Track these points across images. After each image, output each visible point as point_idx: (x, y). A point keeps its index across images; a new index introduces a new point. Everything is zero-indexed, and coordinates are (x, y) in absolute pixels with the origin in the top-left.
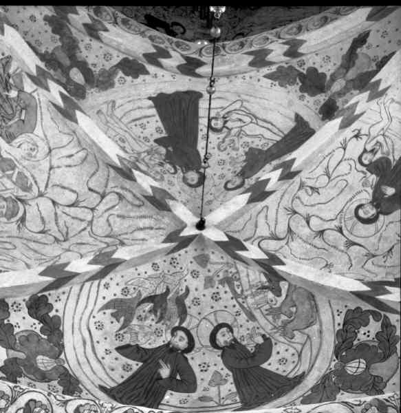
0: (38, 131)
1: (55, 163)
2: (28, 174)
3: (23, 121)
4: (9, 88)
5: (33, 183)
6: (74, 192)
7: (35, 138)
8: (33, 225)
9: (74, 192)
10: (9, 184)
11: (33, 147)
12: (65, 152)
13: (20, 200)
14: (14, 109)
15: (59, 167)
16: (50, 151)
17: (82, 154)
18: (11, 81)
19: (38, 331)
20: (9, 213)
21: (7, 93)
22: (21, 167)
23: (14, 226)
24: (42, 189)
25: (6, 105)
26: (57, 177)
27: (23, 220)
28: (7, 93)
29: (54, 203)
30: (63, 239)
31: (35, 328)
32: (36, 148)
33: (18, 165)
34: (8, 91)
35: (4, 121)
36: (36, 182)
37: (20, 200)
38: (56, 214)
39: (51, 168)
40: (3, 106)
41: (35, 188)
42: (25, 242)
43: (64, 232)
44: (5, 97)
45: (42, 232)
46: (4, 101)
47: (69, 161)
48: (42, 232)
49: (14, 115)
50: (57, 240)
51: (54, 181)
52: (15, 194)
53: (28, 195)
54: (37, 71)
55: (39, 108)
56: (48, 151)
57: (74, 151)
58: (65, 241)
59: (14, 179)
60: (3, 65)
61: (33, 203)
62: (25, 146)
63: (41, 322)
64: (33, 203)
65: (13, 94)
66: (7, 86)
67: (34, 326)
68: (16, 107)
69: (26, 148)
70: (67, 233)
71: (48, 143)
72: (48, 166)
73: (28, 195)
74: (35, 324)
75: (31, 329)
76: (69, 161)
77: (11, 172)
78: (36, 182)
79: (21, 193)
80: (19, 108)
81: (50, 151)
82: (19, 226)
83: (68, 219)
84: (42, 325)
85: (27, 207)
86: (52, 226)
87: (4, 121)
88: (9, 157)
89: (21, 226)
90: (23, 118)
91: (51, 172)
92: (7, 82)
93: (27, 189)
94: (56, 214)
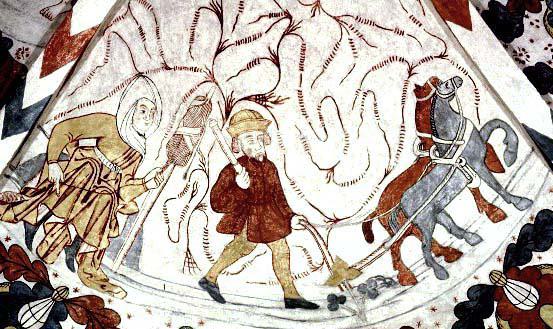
0: (109, 106)
1: (157, 62)
2: (184, 108)
3: (98, 139)
4: (46, 185)
5: (193, 96)
6: (197, 15)
7: (124, 108)
8: (261, 80)
9: (197, 15)
10: (208, 139)
11: (140, 109)
12: (137, 47)
13: (228, 113)
14: (83, 162)
15: (162, 54)
16: (140, 75)
17: (139, 10)
18: (33, 184)
19: (539, 16)
20: (255, 124)
21: (57, 186)
22: (175, 125)
23: (276, 110)
24: (201, 76)
25: (81, 179)
26: (176, 52)
27: (261, 99)
28: (57, 186)
29: (219, 51)
30: (288, 21)
31: (538, 21)
32: (139, 105)
33: (173, 130)
34: (52, 184)
35: (106, 177)
36: (192, 91)
37: (228, 113)
38: (238, 43)
39: (168, 68)
40: (81, 186)
41: (200, 92)
42: (306, 84)
43: (268, 21)
44: (65, 188)
45: (276, 60)
46: (71, 188)
47: (150, 34)
48: (276, 60)
49: (90, 161)
50: (289, 32)
51: (184, 58)
52: (221, 123)
53: (216, 98)
54: (16, 132)
55: (71, 115)
56: (141, 79)
57: (134, 28)
58: (290, 17)
59: (198, 131)
60: (8, 209)
61: (227, 89)
62: (140, 125)
63: (523, 15)
64: (227, 89)
65: (55, 172)
66: (45, 189)
67: (536, 23)
68: (76, 160)
69: (143, 121)
70: (271, 16)
71: (129, 81)
72: (163, 74)
73: (216, 98)
74: (532, 24)
75: (542, 28)
76: (150, 34)
77: (187, 139)
78: (192, 91)
79: (217, 113)
80: (78, 155)
81: (140, 75)
82: (276, 102)
83: (244, 19)
84: (526, 12)
85: (237, 96)
86: (259, 49)
87: (106, 177)
88: (164, 151)
89: (273, 99)
90: (93, 142)
91: (171, 66)
92: (37, 192)
93: (206, 103)
94: (238, 43)
